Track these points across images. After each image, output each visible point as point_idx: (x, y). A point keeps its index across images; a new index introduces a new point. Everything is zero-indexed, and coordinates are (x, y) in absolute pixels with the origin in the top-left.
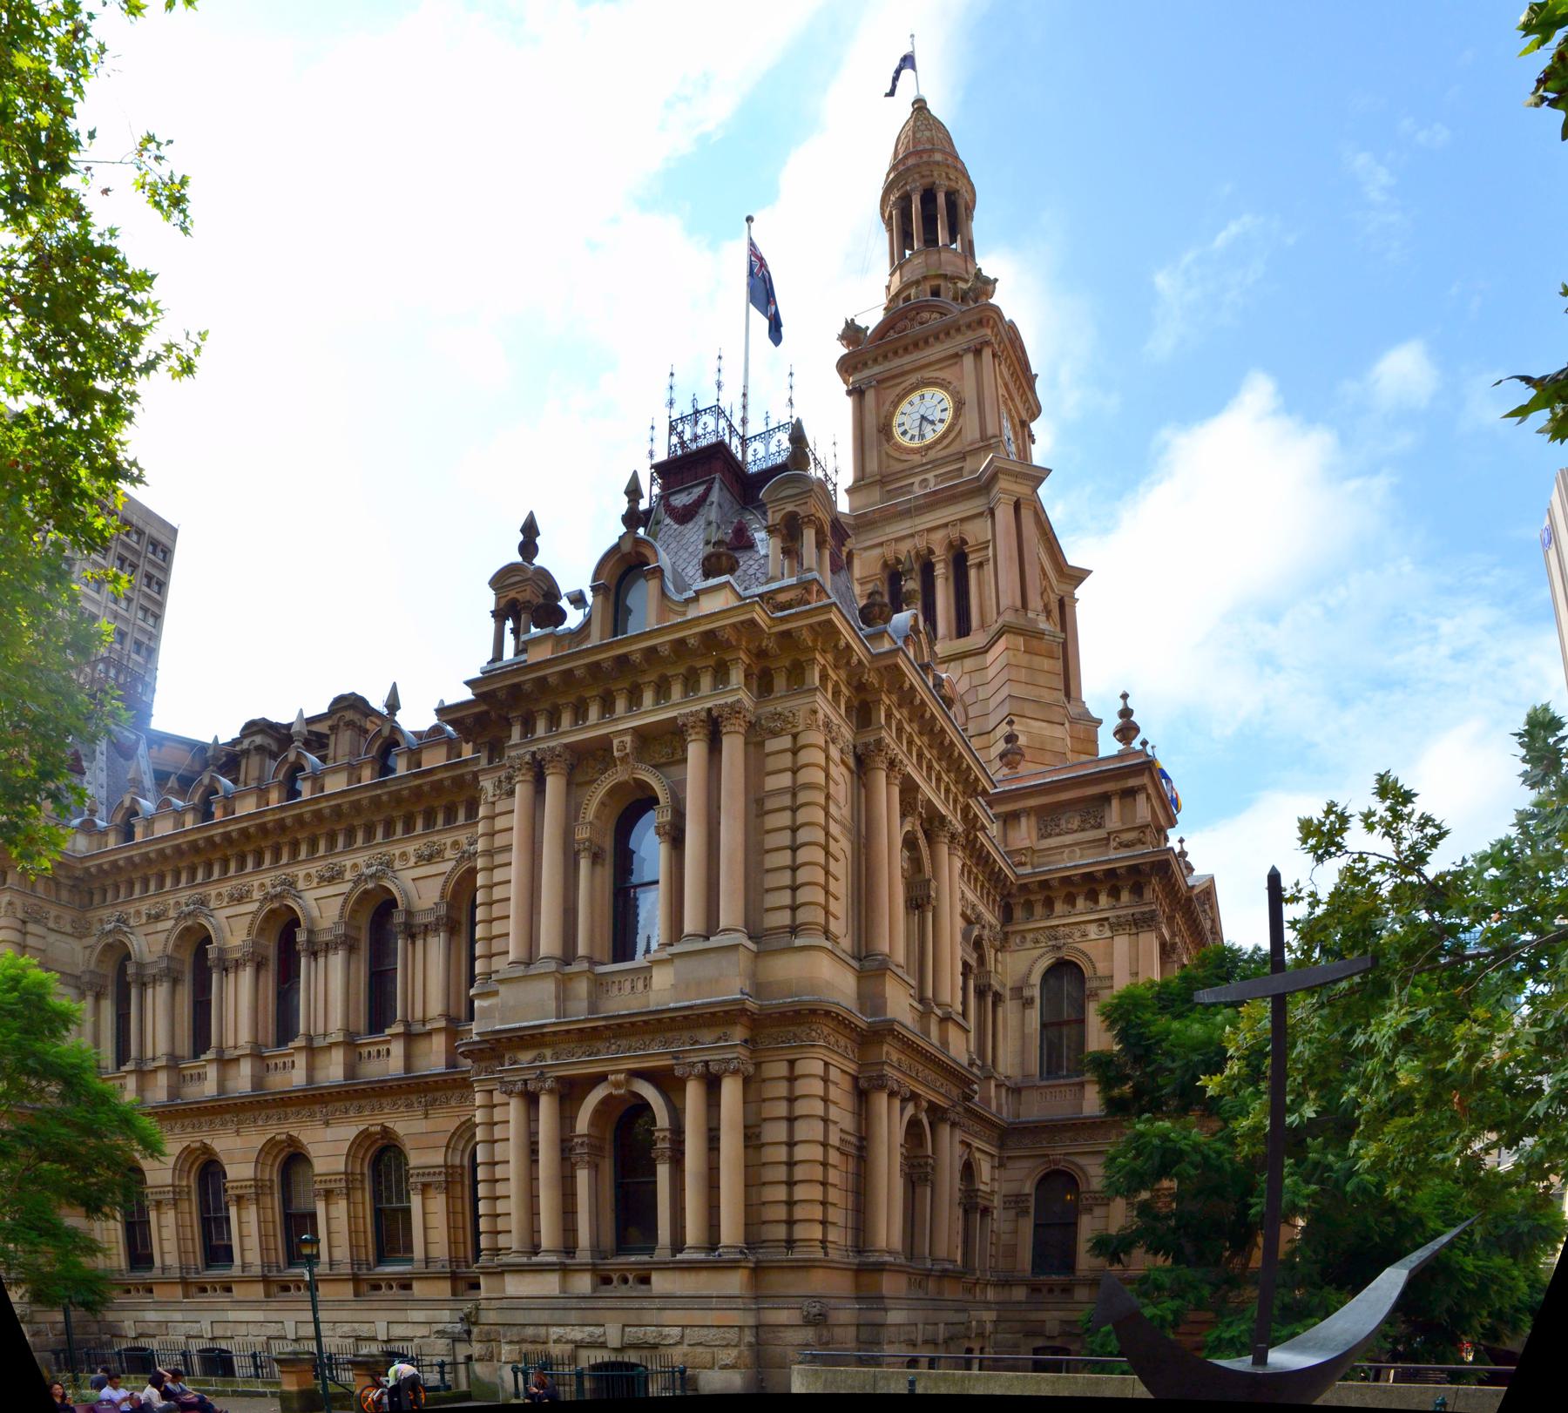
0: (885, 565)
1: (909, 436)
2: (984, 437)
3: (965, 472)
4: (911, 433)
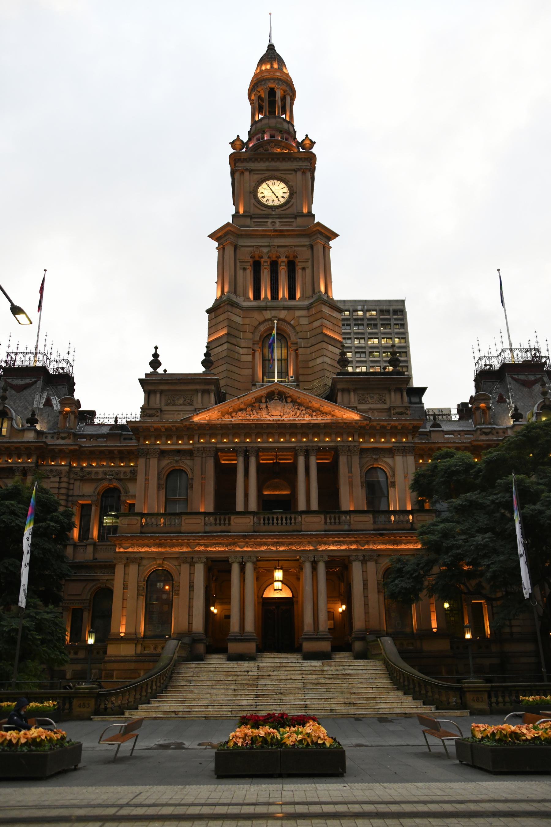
3: (294, 224)
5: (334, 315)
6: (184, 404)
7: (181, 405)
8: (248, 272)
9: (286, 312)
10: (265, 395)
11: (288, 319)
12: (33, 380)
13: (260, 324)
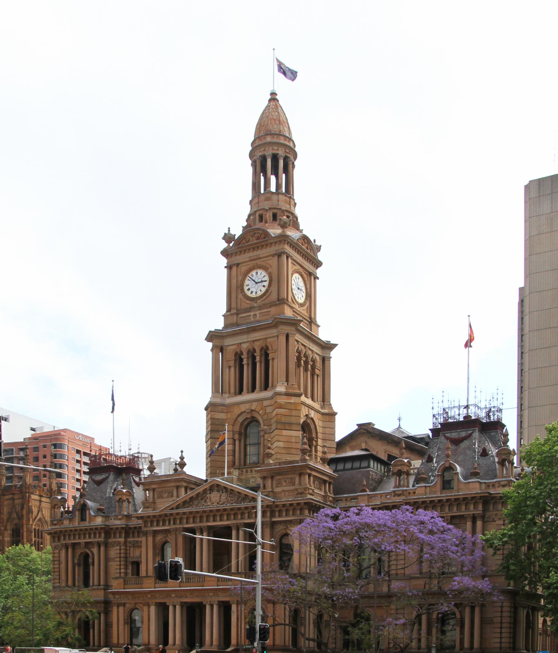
0: (236, 354)
1: (250, 291)
2: (278, 300)
4: (251, 290)
5: (292, 401)
6: (168, 497)
7: (166, 498)
8: (232, 369)
9: (256, 403)
10: (208, 488)
11: (258, 410)
12: (107, 475)
13: (239, 416)
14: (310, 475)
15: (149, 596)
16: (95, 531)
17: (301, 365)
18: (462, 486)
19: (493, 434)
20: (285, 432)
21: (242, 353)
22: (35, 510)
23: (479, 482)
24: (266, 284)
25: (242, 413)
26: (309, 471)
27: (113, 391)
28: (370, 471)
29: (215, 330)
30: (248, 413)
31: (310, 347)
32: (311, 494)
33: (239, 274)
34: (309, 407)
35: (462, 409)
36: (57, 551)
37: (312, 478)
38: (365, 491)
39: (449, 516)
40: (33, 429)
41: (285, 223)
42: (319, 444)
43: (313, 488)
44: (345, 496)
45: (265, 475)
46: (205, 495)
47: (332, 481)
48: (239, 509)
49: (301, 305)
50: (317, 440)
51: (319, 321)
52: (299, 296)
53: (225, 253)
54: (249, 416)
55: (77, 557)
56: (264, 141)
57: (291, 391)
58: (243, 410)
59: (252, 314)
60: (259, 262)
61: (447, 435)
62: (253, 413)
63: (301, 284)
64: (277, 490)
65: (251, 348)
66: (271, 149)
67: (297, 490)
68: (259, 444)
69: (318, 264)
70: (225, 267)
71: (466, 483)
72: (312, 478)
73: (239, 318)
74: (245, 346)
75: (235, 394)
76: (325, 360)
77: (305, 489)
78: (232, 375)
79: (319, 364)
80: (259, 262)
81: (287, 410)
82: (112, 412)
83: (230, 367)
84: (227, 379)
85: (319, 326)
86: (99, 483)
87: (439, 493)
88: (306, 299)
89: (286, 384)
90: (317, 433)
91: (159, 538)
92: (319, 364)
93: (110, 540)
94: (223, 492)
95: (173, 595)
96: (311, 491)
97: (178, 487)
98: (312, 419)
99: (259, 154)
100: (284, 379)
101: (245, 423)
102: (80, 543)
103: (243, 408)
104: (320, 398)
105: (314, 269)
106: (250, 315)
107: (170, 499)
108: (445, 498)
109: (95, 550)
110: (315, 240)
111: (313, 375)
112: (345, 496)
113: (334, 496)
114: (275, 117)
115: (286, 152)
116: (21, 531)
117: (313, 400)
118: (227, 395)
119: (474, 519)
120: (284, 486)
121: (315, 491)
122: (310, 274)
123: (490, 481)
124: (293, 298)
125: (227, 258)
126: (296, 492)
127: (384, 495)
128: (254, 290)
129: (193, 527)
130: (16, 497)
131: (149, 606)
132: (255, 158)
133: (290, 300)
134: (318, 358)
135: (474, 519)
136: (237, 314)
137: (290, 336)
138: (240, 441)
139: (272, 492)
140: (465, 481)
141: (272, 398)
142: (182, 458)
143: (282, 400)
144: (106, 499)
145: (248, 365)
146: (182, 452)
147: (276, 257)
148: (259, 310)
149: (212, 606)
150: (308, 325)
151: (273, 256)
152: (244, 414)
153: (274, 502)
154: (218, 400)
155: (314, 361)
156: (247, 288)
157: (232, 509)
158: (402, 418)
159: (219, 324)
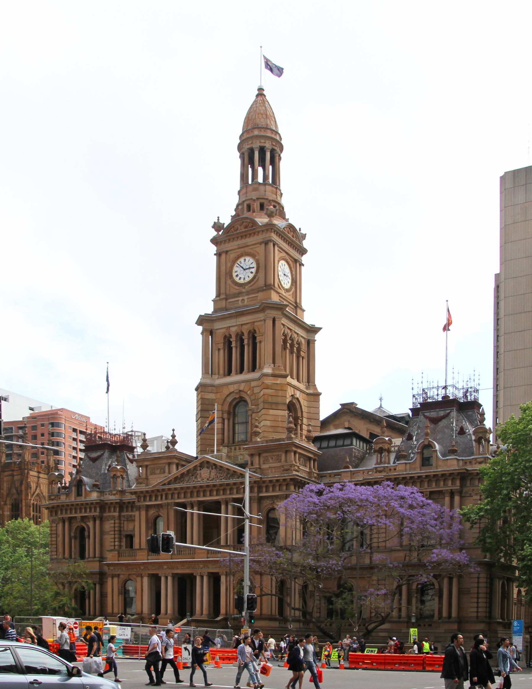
0: (225, 337)
1: (238, 277)
2: (265, 286)
4: (240, 276)
5: (278, 382)
6: (160, 473)
8: (222, 351)
9: (245, 384)
10: (199, 465)
12: (102, 452)
13: (228, 396)
14: (295, 453)
15: (142, 568)
16: (91, 505)
17: (287, 348)
18: (440, 463)
19: (470, 413)
20: (272, 412)
21: (230, 336)
22: (33, 486)
23: (456, 459)
24: (254, 270)
25: (231, 393)
26: (294, 449)
27: (107, 372)
28: (352, 448)
29: (205, 314)
30: (237, 393)
31: (296, 331)
32: (296, 471)
33: (228, 261)
34: (295, 387)
35: (440, 390)
36: (54, 525)
37: (297, 455)
38: (348, 468)
39: (428, 491)
40: (31, 409)
41: (272, 212)
42: (304, 423)
43: (298, 464)
44: (329, 472)
45: (253, 453)
46: (195, 471)
47: (315, 458)
48: (228, 485)
49: (287, 291)
50: (303, 419)
51: (304, 305)
52: (285, 282)
53: (214, 241)
54: (237, 396)
55: (73, 530)
56: (251, 135)
57: (277, 372)
58: (232, 390)
59: (240, 299)
60: (247, 249)
61: (426, 414)
62: (242, 393)
63: (287, 271)
64: (264, 466)
65: (239, 331)
66: (258, 142)
67: (283, 466)
68: (247, 423)
69: (303, 252)
70: (215, 254)
71: (444, 460)
72: (297, 455)
73: (228, 303)
74: (233, 329)
75: (225, 375)
76: (310, 343)
77: (291, 466)
78: (221, 357)
79: (304, 347)
80: (247, 249)
81: (273, 391)
82: (107, 392)
83: (219, 350)
84: (217, 361)
85: (304, 311)
86: (94, 460)
87: (419, 469)
88: (292, 285)
89: (272, 365)
90: (302, 412)
91: (152, 512)
92: (304, 347)
93: (105, 515)
94: (212, 469)
95: (165, 567)
96: (296, 468)
97: (169, 464)
98: (297, 399)
99: (247, 146)
100: (271, 361)
101: (234, 403)
102: (76, 517)
103: (232, 388)
104: (305, 379)
105: (299, 256)
106: (238, 300)
107: (163, 475)
108: (424, 474)
109: (91, 524)
110: (300, 229)
111: (298, 357)
112: (329, 472)
113: (318, 473)
114: (262, 112)
115: (273, 145)
116: (20, 506)
117: (298, 381)
118: (217, 376)
119: (452, 494)
120: (270, 463)
121: (300, 468)
122: (296, 261)
123: (467, 458)
124: (279, 284)
125: (216, 246)
126: (282, 469)
127: (366, 472)
128: (242, 277)
129: (184, 502)
130: (15, 474)
131: (142, 577)
132: (243, 150)
133: (276, 285)
134: (303, 341)
135: (452, 494)
136: (226, 299)
137: (276, 320)
138: (229, 420)
139: (260, 468)
140: (444, 458)
141: (259, 379)
142: (173, 436)
143: (269, 381)
144: (101, 475)
145: (236, 347)
146: (173, 430)
147: (263, 245)
148: (247, 295)
149: (202, 577)
150: (293, 309)
151: (261, 243)
152: (232, 395)
153: (261, 478)
154: (208, 381)
155: (299, 344)
156: (236, 274)
157: (221, 485)
158: (384, 398)
159: (209, 309)
